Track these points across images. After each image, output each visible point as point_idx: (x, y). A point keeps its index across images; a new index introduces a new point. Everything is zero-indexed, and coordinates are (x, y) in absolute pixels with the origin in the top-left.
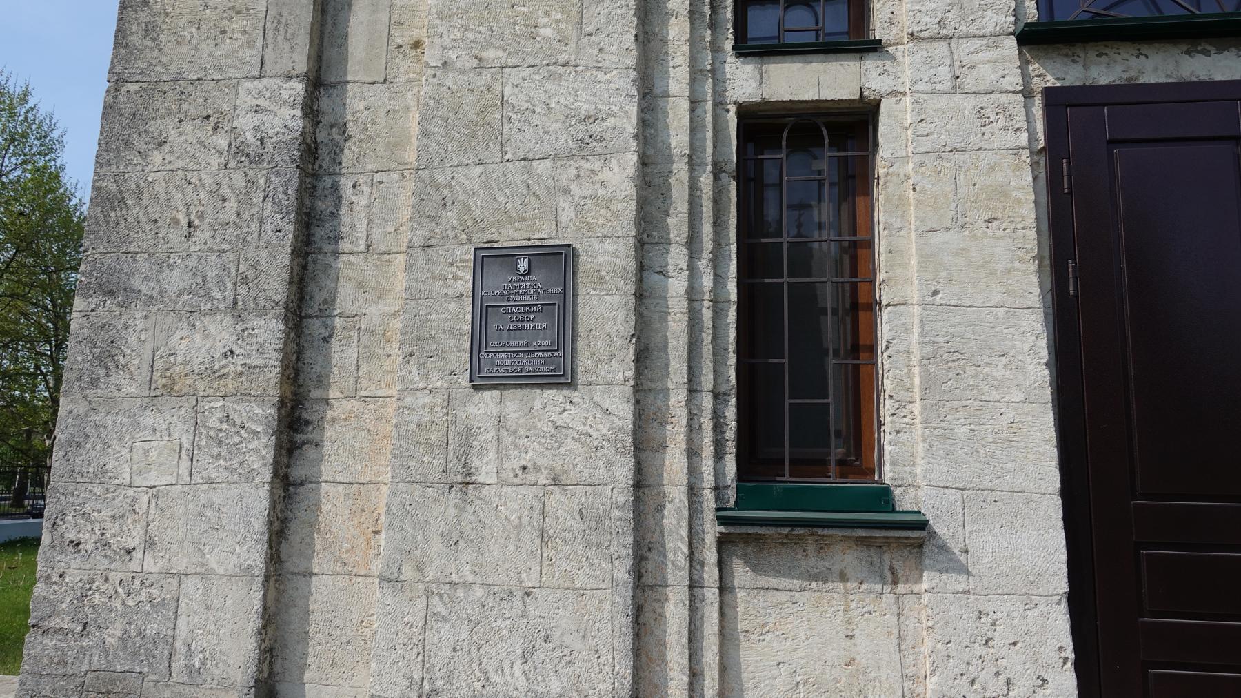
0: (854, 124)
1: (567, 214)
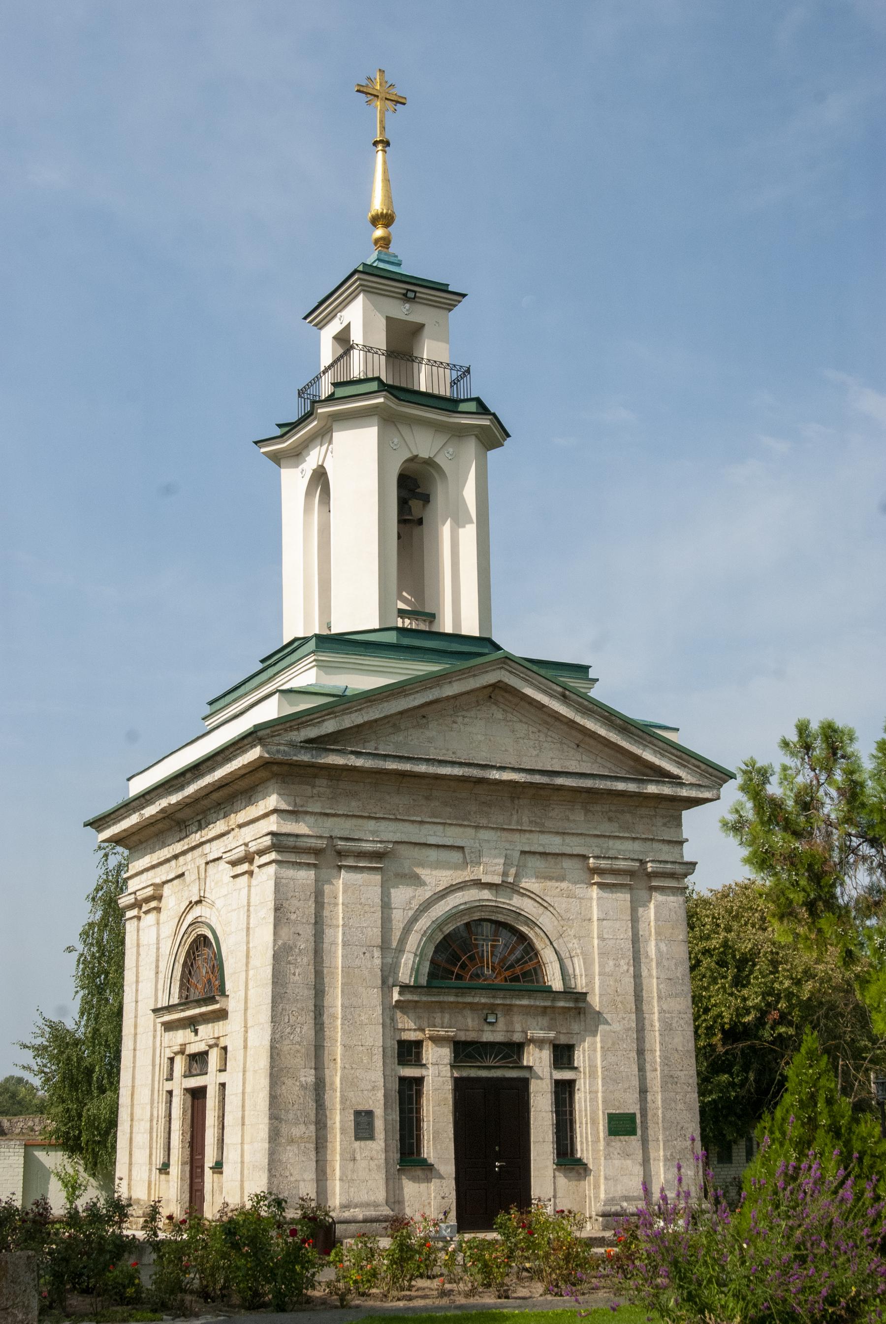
0: (419, 1081)
1: (371, 1102)
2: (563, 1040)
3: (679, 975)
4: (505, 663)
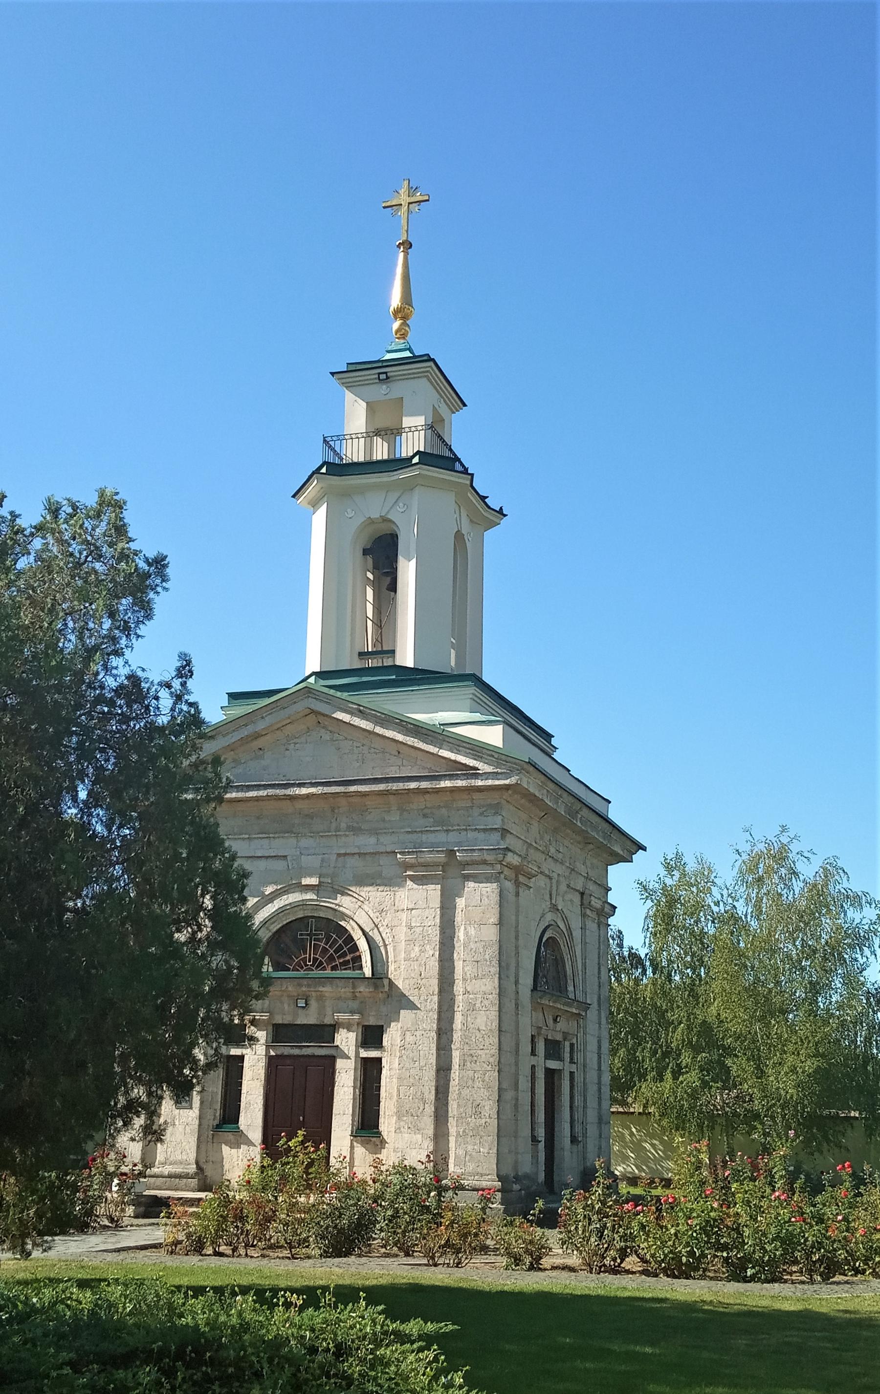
2: (372, 1021)
3: (487, 957)
4: (310, 692)
